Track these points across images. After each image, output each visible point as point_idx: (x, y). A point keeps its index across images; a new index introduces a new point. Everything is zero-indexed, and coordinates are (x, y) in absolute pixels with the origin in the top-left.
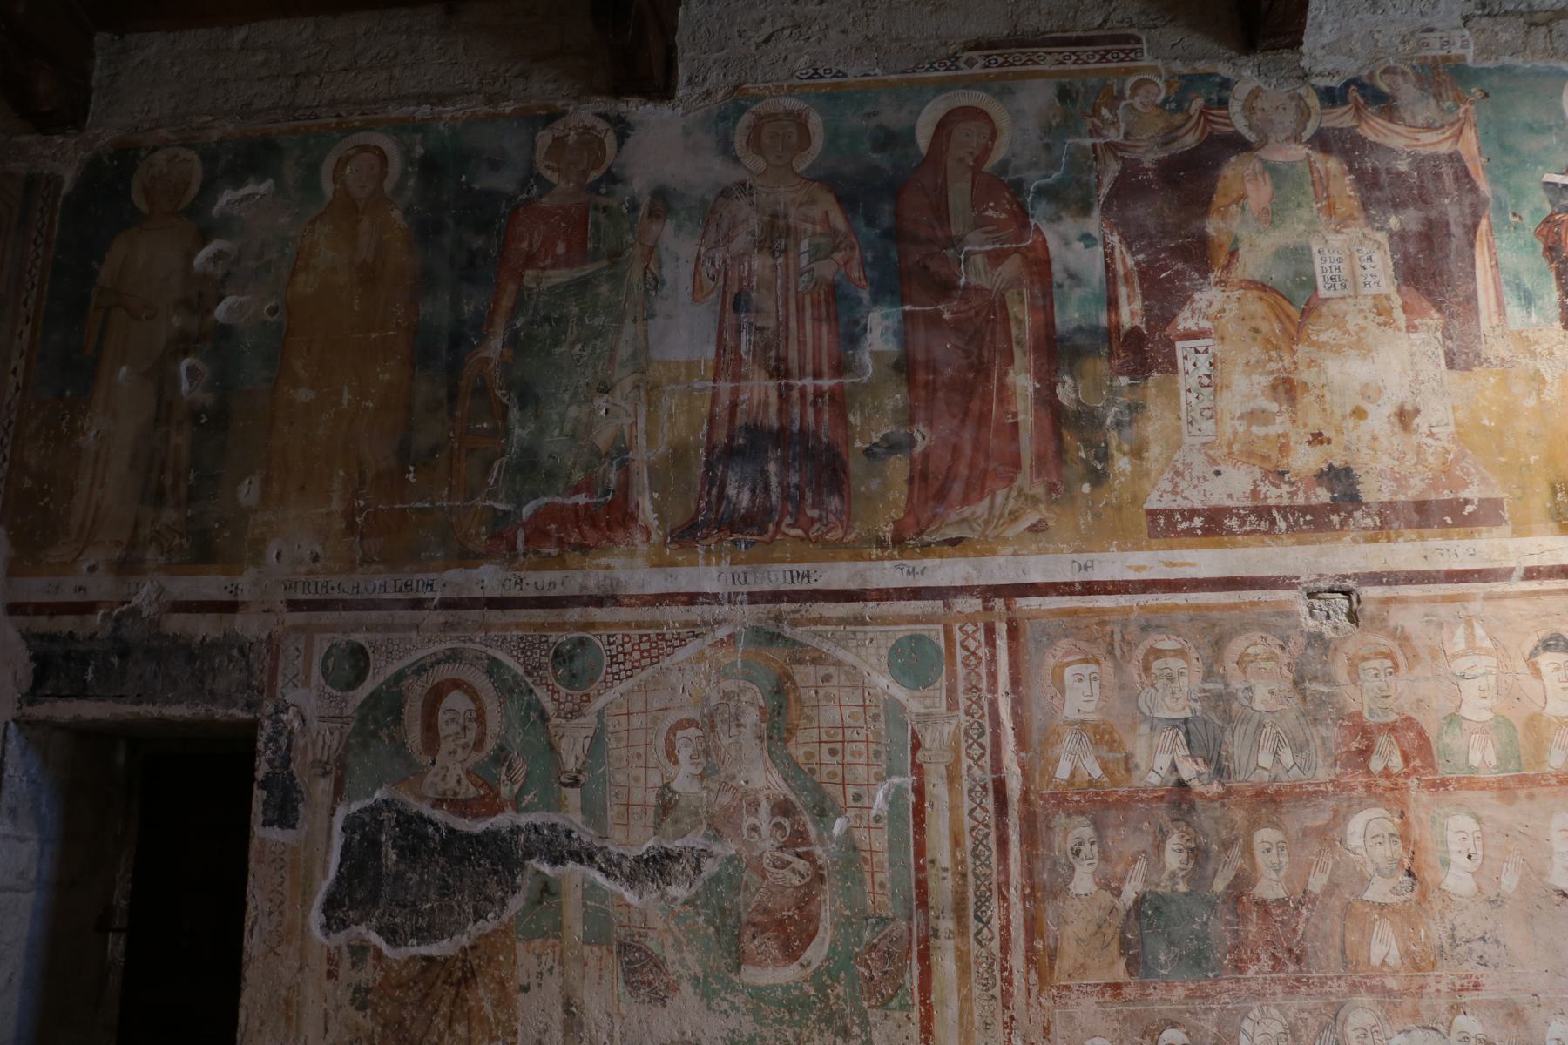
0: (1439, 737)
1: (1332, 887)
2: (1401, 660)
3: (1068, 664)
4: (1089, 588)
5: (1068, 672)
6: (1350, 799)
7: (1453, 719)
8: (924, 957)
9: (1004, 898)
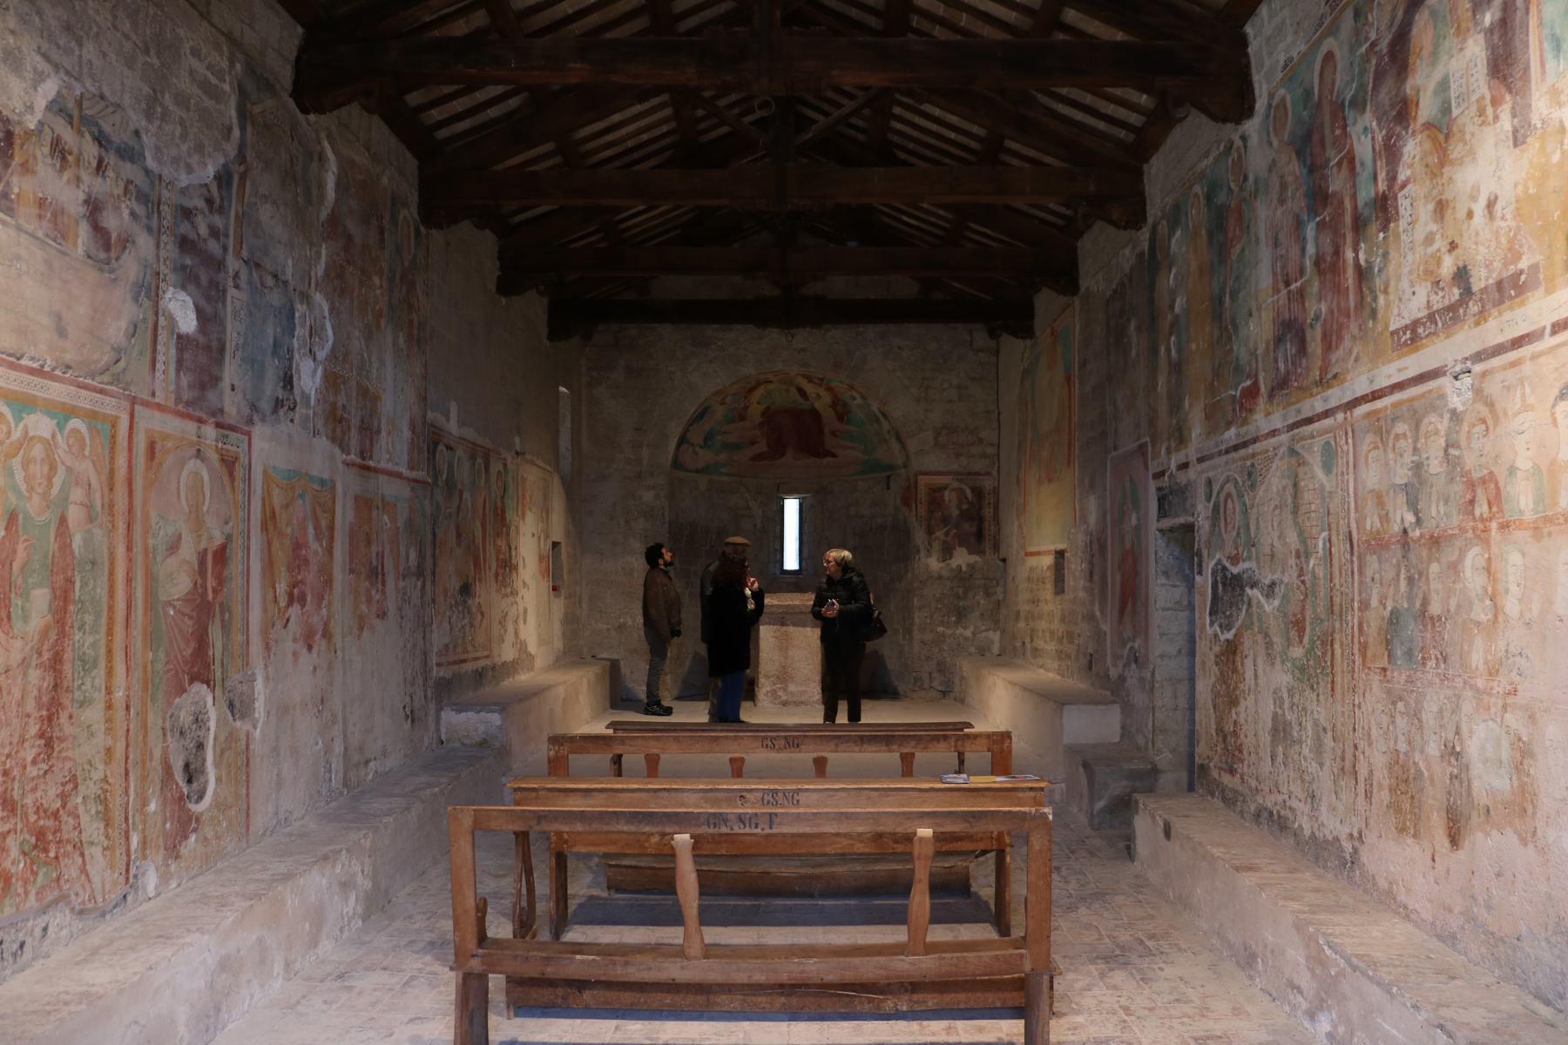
0: (1505, 487)
1: (1459, 606)
2: (1490, 423)
3: (1369, 451)
4: (1376, 395)
5: (1370, 455)
6: (1466, 539)
7: (1512, 470)
8: (1332, 645)
9: (1353, 609)
